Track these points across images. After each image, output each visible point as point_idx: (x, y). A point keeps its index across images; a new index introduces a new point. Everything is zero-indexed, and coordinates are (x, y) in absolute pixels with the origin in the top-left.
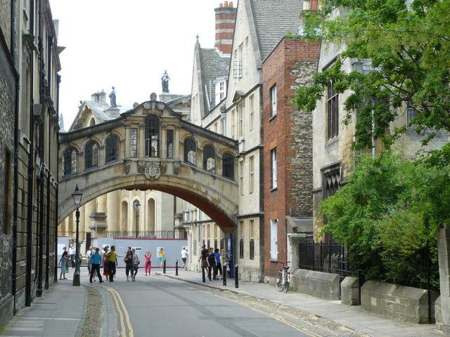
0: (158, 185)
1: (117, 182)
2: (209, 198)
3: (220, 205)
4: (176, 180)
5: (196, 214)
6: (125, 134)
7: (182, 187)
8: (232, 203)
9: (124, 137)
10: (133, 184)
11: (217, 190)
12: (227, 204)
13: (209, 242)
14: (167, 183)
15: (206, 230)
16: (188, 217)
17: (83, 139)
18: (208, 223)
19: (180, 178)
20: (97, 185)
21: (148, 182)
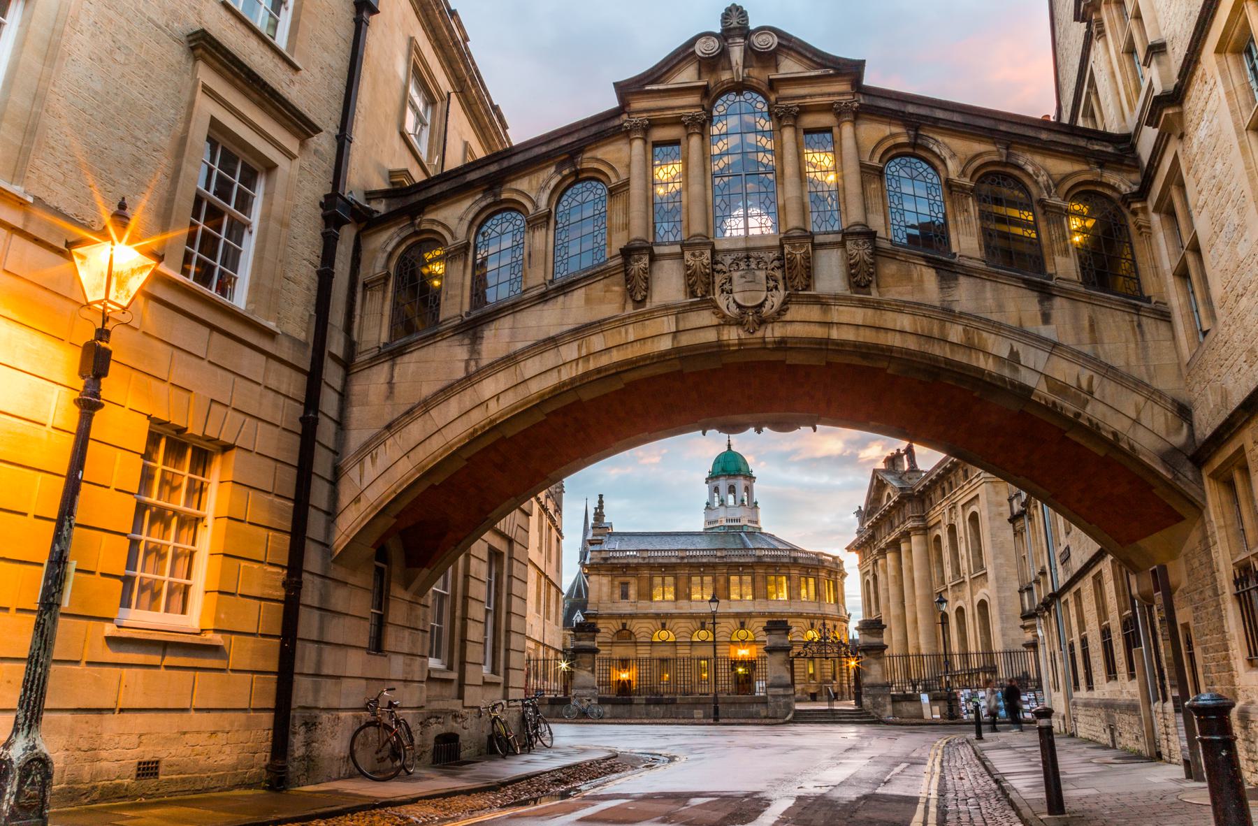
0: (782, 344)
1: (597, 342)
2: (1029, 379)
3: (1095, 411)
4: (859, 315)
5: (1046, 584)
6: (629, 166)
7: (895, 341)
8: (1154, 395)
9: (624, 177)
10: (665, 344)
11: (1069, 340)
12: (1129, 402)
13: (1084, 641)
14: (819, 332)
15: (1073, 611)
16: (1031, 599)
17: (467, 203)
18: (1074, 589)
19: (878, 306)
20: (510, 360)
21: (732, 335)
